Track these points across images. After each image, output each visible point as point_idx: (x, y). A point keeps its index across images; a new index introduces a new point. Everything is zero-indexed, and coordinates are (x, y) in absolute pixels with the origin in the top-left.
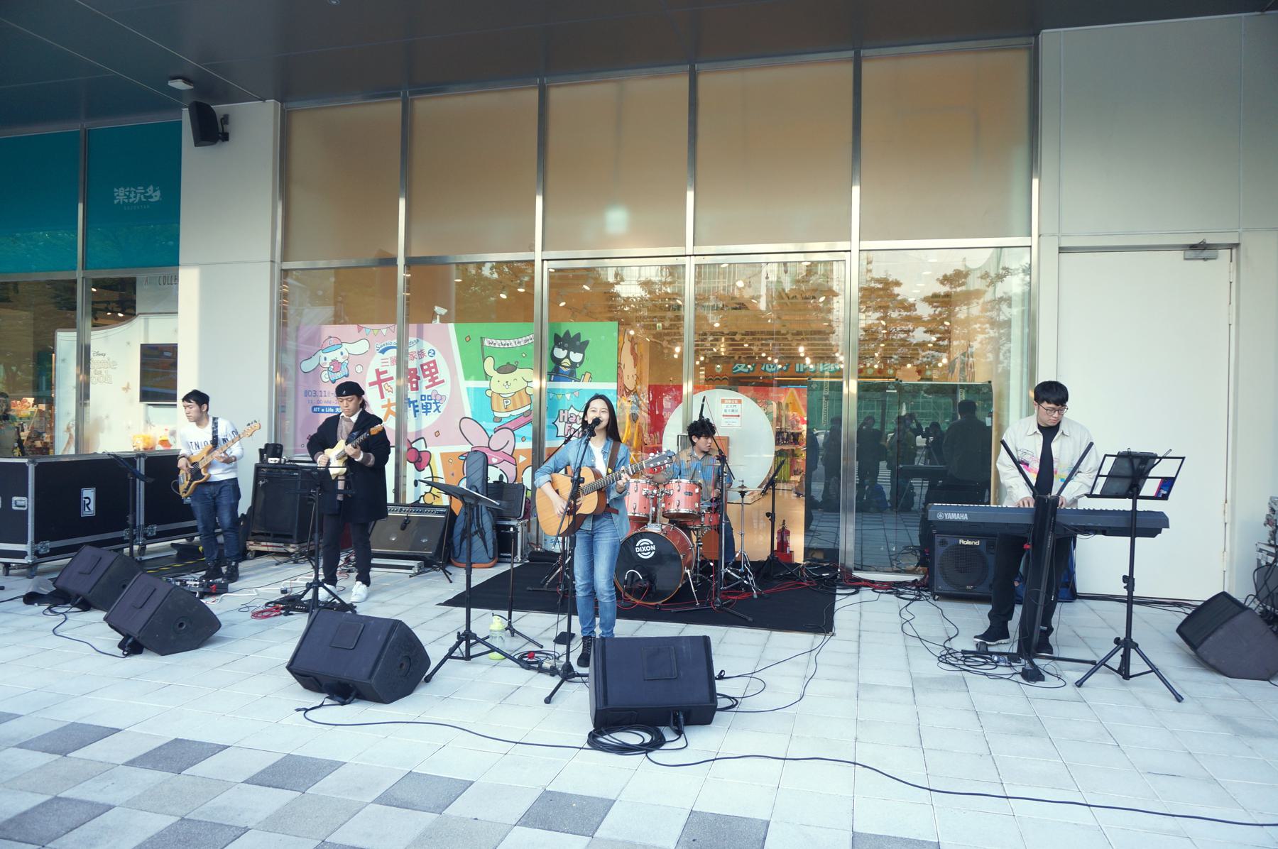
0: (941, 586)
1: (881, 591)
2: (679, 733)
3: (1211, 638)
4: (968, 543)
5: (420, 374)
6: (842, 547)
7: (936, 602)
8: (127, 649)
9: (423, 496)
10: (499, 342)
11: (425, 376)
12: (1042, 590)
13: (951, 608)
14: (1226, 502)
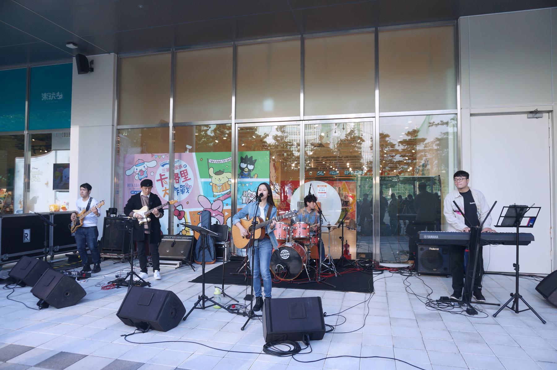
0: (421, 269)
1: (393, 272)
2: (307, 344)
3: (554, 292)
4: (433, 249)
5: (180, 176)
6: (374, 252)
7: (419, 277)
8: (41, 306)
9: (181, 231)
10: (216, 161)
11: (182, 177)
12: (474, 271)
13: (427, 279)
14: (551, 228)
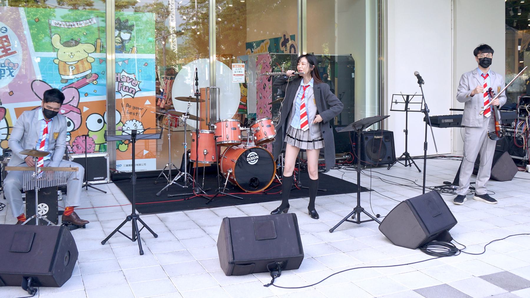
4: (378, 137)
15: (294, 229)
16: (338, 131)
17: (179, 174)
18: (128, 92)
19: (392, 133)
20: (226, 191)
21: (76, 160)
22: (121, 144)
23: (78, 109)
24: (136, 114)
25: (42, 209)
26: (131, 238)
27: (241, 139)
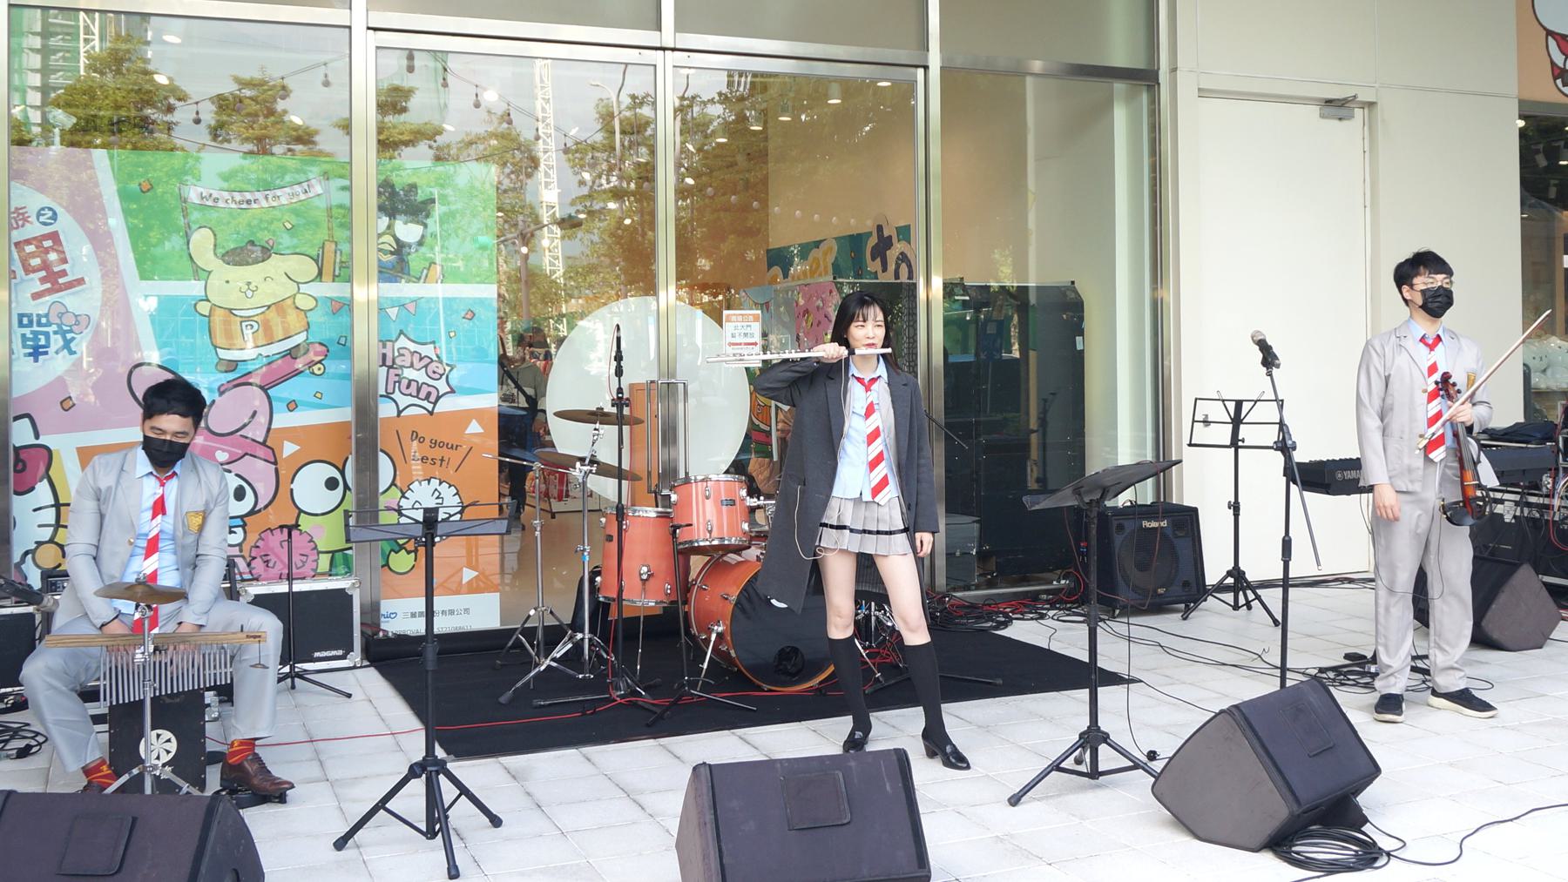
15: (903, 795)
16: (1032, 506)
17: (566, 639)
18: (417, 397)
19: (1194, 511)
20: (706, 688)
21: (261, 601)
22: (396, 553)
23: (268, 448)
24: (438, 463)
25: (159, 747)
26: (424, 828)
27: (751, 532)
